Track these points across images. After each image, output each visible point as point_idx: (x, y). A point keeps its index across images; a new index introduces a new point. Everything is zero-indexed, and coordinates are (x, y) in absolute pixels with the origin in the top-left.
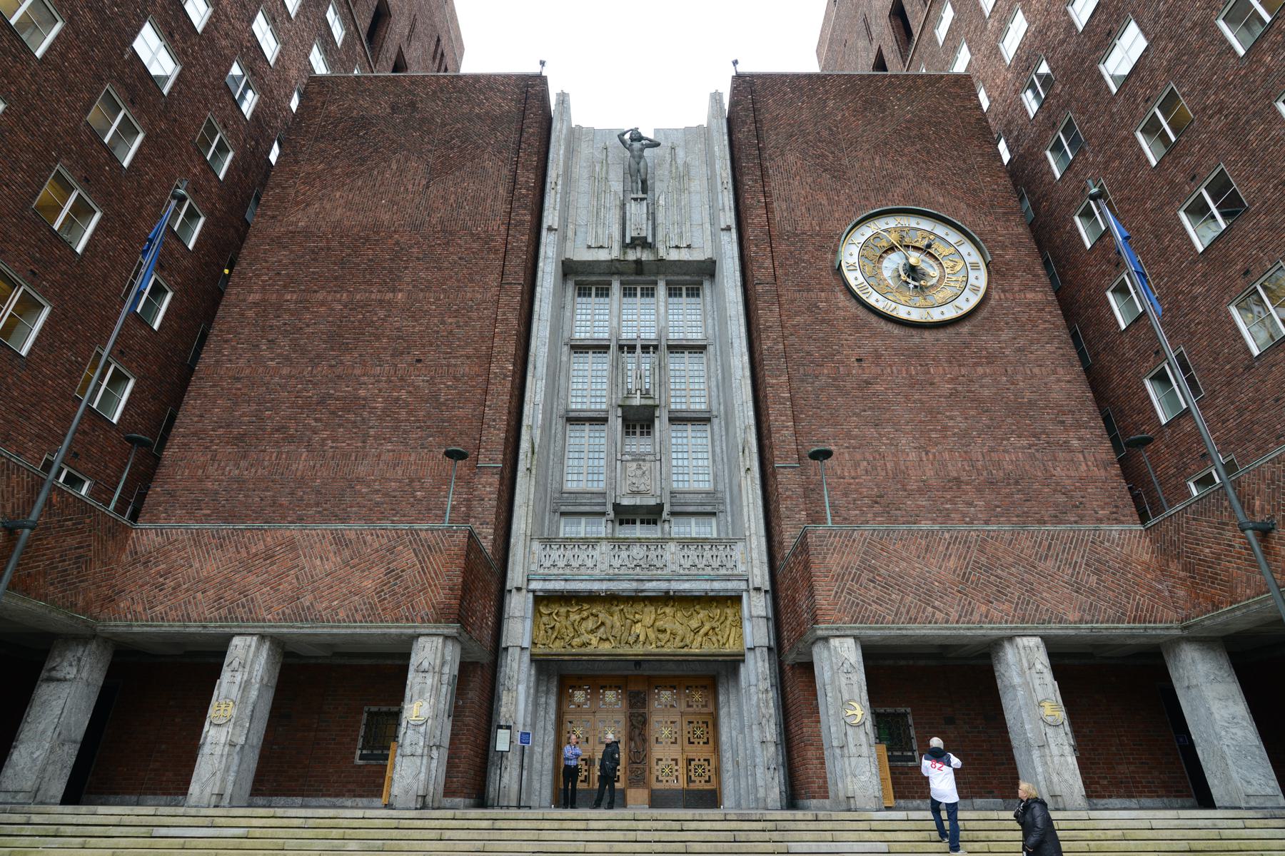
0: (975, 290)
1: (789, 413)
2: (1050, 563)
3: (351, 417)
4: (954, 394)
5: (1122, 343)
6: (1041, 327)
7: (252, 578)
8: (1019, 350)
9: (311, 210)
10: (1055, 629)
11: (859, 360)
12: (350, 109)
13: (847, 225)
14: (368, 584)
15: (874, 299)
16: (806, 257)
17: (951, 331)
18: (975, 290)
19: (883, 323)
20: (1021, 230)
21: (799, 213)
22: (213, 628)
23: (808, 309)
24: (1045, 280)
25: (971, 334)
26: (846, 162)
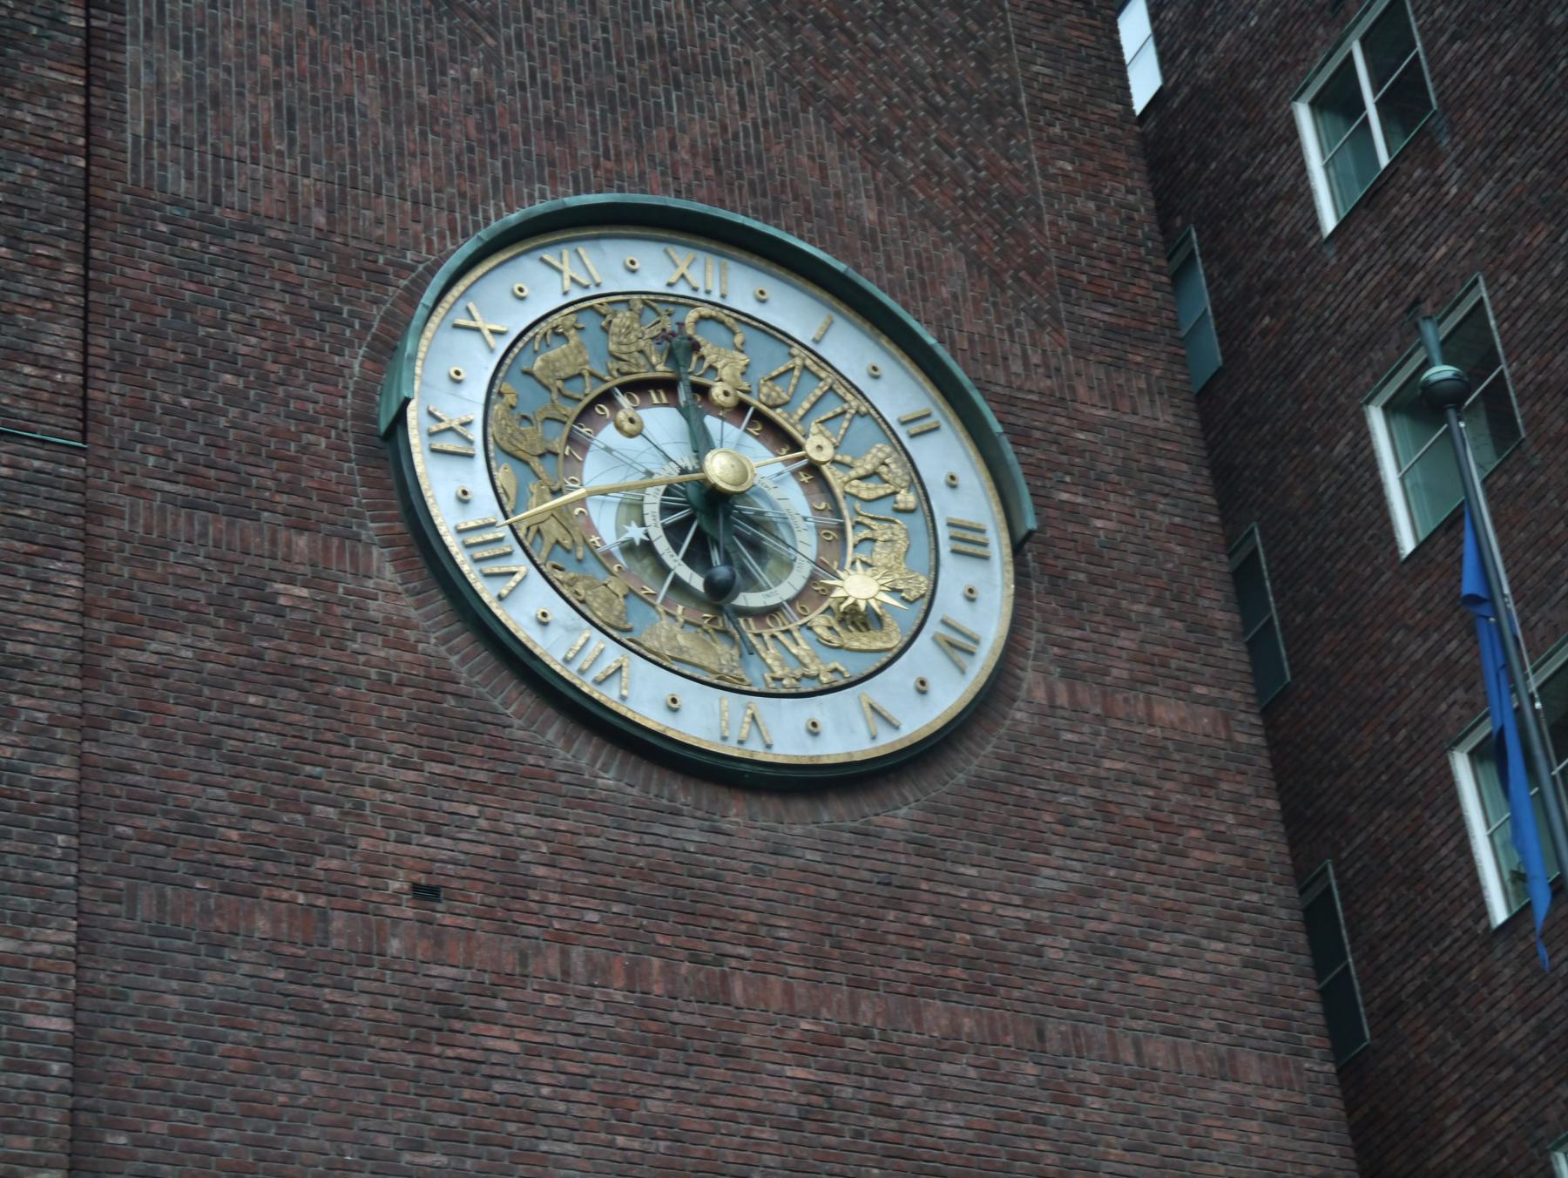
0: (958, 647)
1: (52, 1118)
5: (1487, 978)
6: (1198, 857)
8: (1102, 947)
11: (425, 893)
13: (458, 233)
15: (530, 610)
16: (246, 346)
18: (958, 647)
19: (554, 731)
20: (1165, 419)
21: (241, 124)
23: (221, 604)
24: (1232, 652)
25: (922, 847)
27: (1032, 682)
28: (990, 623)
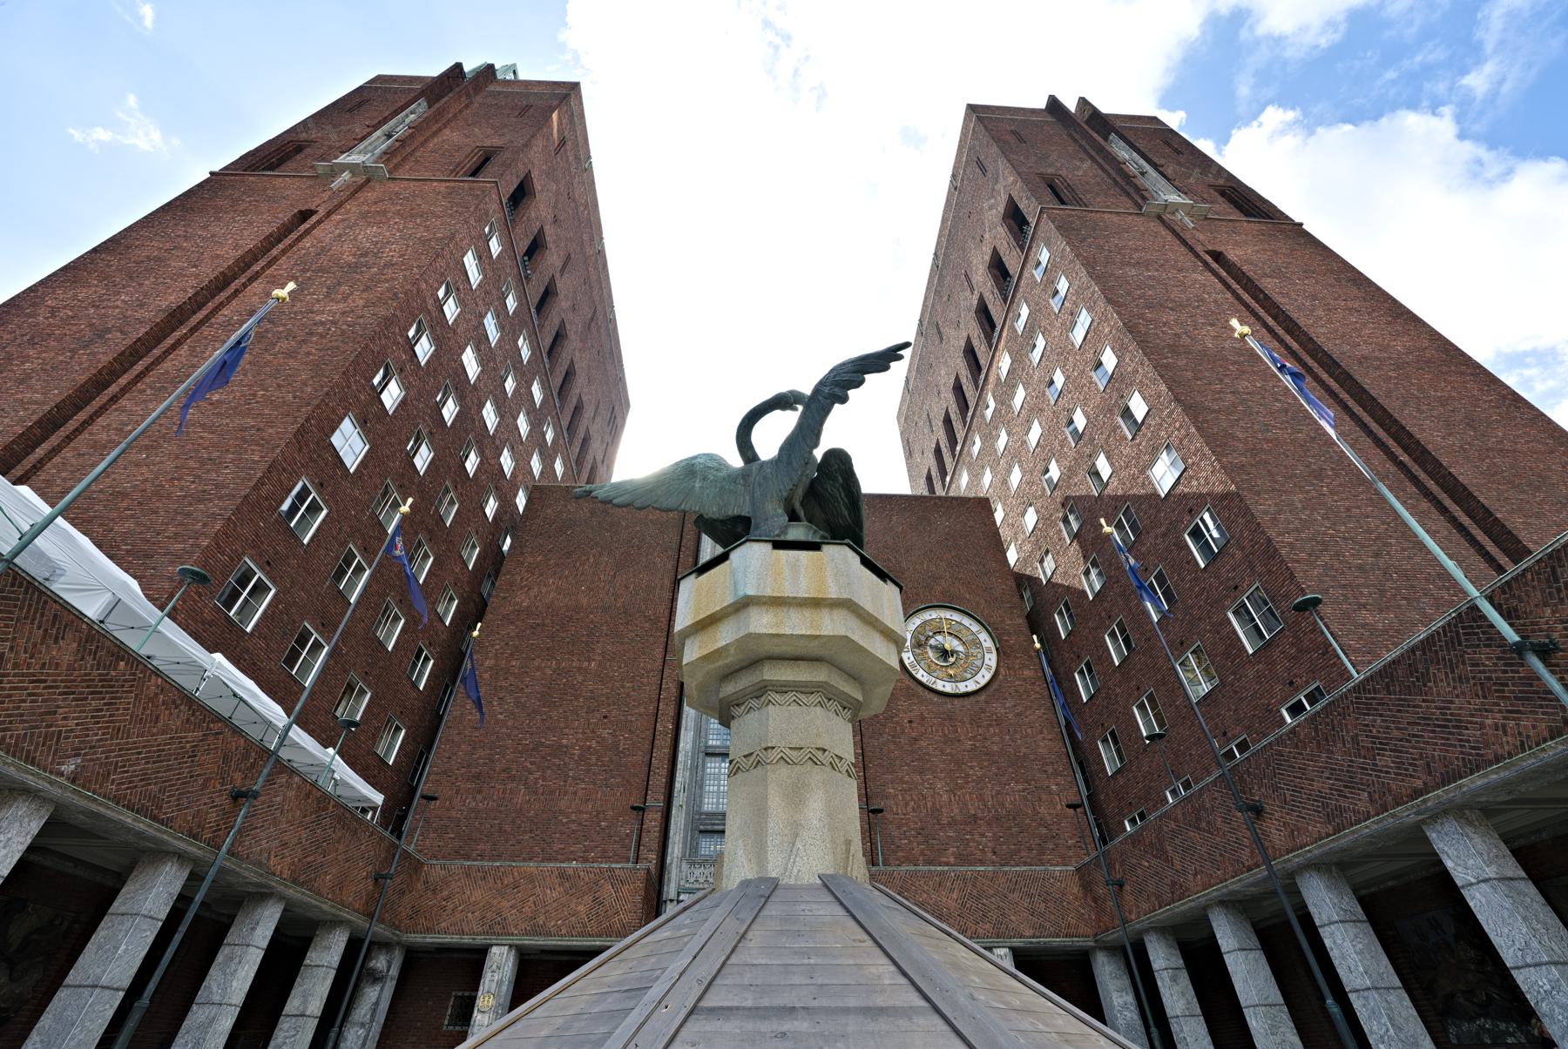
0: (989, 668)
2: (1016, 895)
3: (557, 761)
4: (974, 748)
7: (504, 903)
9: (532, 593)
10: (1017, 942)
12: (561, 512)
14: (581, 908)
17: (972, 698)
18: (989, 668)
22: (480, 940)
26: (904, 565)
27: (1002, 670)
28: (993, 664)
